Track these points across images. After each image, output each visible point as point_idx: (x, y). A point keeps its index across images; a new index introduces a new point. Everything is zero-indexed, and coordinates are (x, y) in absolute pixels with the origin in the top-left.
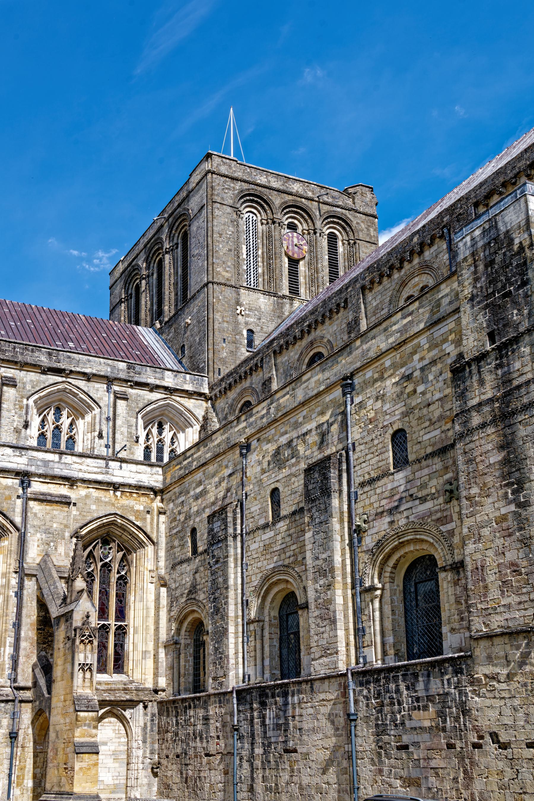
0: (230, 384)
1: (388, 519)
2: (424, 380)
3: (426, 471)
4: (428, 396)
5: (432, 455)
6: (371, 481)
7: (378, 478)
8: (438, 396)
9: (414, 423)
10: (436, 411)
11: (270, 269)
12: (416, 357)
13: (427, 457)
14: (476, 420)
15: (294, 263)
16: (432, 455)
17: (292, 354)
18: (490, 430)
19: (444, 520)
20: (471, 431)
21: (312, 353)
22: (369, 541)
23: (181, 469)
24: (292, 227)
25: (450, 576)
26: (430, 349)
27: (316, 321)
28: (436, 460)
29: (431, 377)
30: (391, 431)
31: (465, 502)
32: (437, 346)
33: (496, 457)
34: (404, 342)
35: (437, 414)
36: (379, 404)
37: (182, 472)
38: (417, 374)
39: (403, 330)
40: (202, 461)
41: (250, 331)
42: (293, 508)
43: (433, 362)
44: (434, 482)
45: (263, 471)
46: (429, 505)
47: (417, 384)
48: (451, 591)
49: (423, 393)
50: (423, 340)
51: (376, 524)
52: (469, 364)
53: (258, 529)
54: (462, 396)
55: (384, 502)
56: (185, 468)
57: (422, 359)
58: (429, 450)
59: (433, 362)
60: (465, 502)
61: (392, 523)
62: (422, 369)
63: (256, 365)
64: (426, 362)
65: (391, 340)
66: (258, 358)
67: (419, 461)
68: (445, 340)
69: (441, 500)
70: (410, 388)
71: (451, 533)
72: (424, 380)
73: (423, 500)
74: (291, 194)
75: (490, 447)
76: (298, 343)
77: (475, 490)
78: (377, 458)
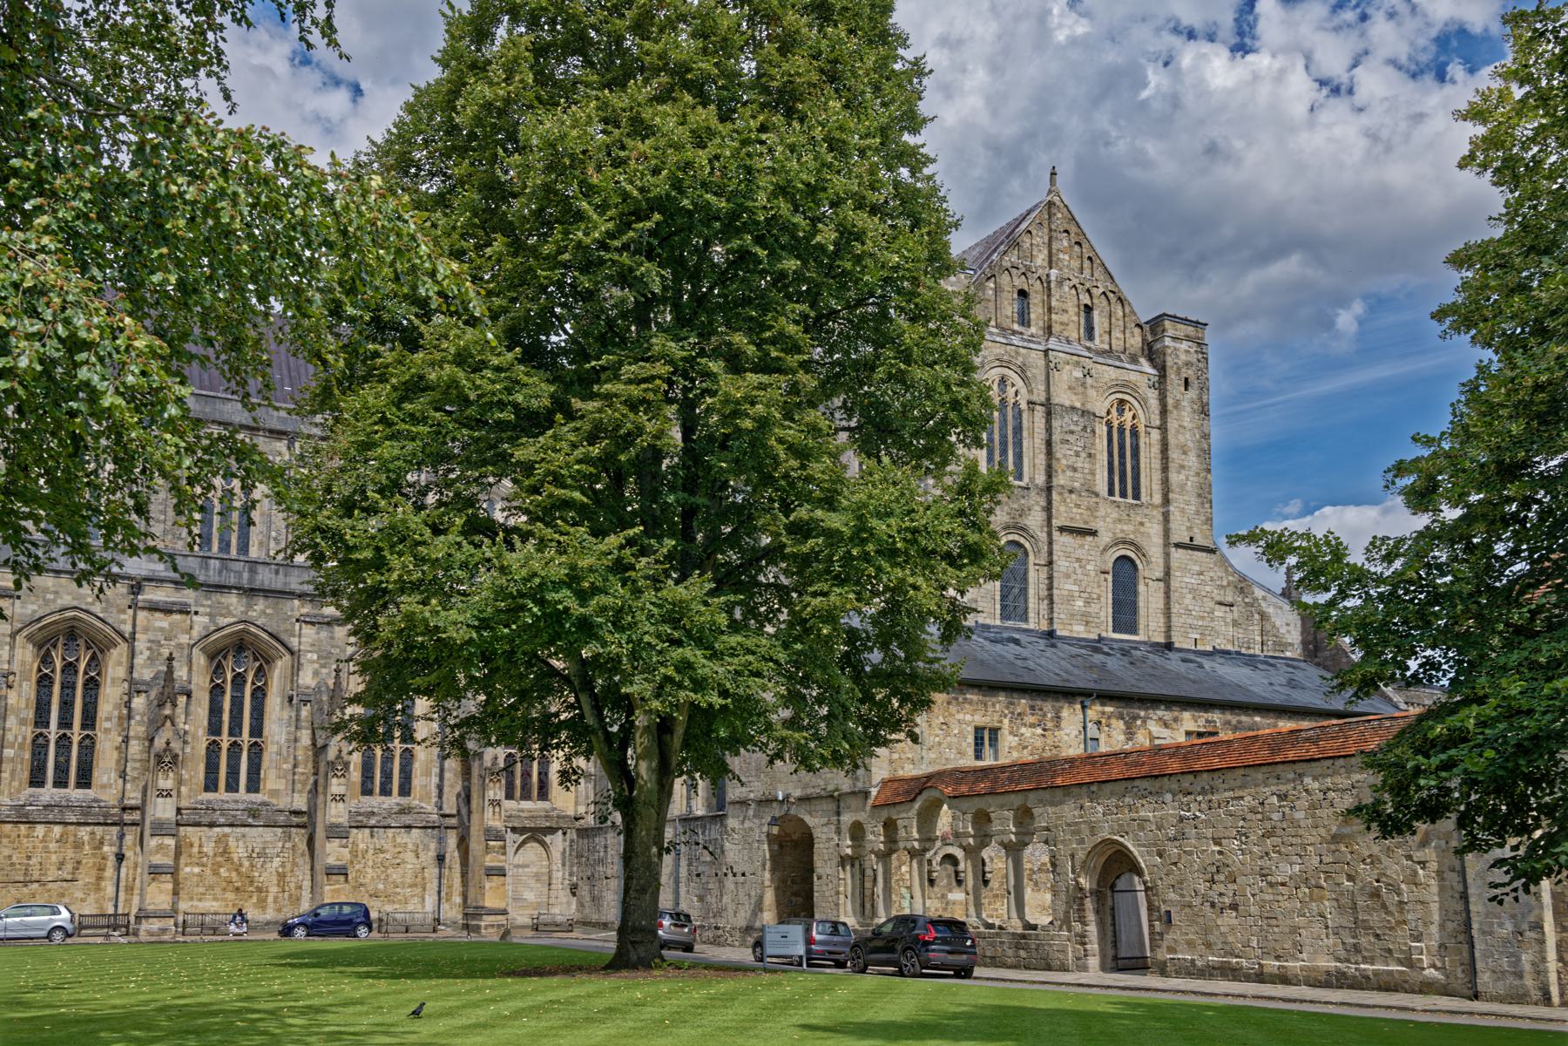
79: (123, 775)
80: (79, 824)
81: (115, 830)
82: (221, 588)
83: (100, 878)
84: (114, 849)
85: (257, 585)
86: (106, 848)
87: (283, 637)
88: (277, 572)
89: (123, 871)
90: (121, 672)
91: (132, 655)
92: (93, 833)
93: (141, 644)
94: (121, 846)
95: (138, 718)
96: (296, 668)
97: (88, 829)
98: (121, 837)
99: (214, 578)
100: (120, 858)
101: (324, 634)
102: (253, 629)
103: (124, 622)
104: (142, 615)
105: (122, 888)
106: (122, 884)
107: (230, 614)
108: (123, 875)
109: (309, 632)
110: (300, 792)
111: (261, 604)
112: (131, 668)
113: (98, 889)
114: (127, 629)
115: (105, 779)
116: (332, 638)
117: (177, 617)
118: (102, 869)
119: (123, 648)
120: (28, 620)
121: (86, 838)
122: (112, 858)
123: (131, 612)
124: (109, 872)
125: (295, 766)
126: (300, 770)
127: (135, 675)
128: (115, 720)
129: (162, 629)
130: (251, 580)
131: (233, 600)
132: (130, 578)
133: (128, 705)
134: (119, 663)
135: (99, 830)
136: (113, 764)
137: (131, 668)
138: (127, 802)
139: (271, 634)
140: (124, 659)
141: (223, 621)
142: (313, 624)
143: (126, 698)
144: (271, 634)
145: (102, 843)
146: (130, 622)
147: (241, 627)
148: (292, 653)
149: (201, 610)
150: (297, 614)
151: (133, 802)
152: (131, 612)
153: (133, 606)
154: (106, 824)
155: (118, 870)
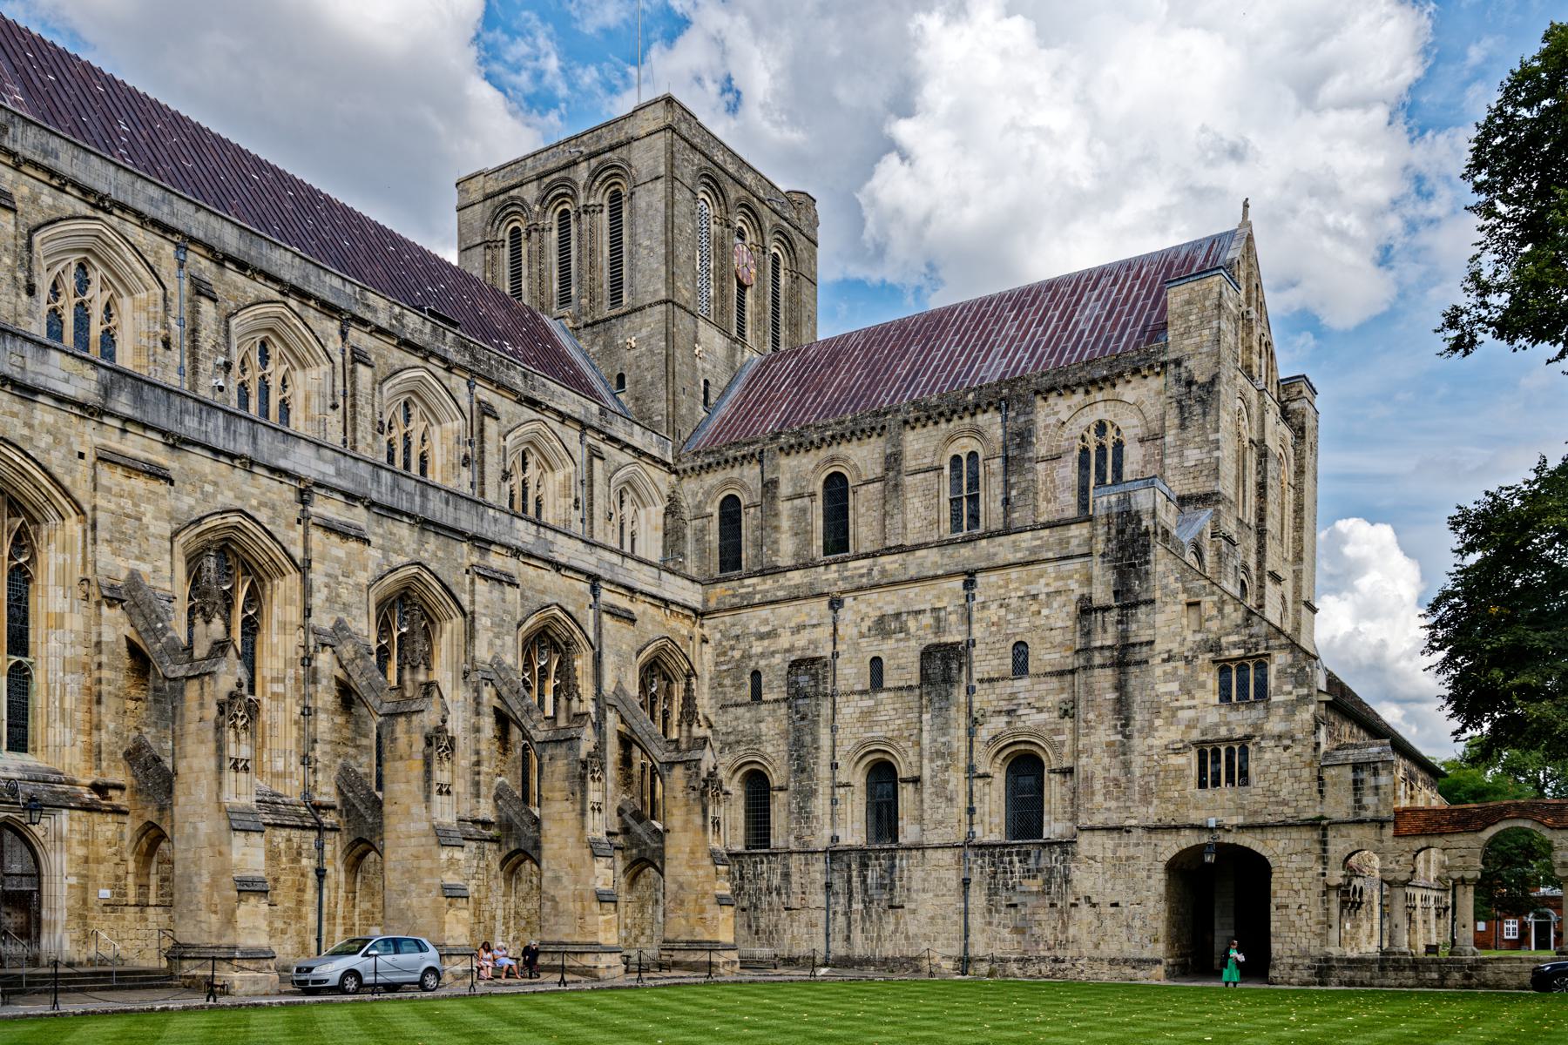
0: (709, 465)
1: (1005, 719)
2: (1049, 605)
3: (1044, 686)
4: (1052, 621)
5: (1051, 674)
6: (990, 680)
7: (997, 680)
8: (1060, 624)
9: (1036, 640)
10: (1057, 637)
11: (722, 294)
12: (1042, 581)
13: (1046, 674)
14: (1098, 659)
15: (742, 287)
16: (1051, 674)
17: (804, 461)
18: (1109, 671)
19: (1057, 732)
20: (1092, 667)
21: (831, 470)
22: (984, 733)
23: (734, 596)
24: (741, 235)
25: (1058, 777)
26: (1057, 579)
27: (843, 436)
28: (1054, 679)
29: (1055, 605)
30: (1013, 641)
31: (1082, 724)
32: (1062, 578)
33: (1112, 695)
34: (1032, 563)
35: (1059, 639)
36: (1002, 612)
37: (736, 600)
38: (1042, 597)
39: (1032, 550)
40: (770, 597)
41: (706, 382)
42: (901, 684)
43: (1058, 592)
44: (1050, 698)
45: (862, 636)
46: (1044, 716)
47: (1042, 605)
48: (1058, 789)
49: (1047, 617)
50: (1050, 567)
51: (994, 720)
52: (1096, 610)
53: (853, 693)
54: (1087, 634)
55: (1002, 703)
56: (743, 597)
57: (1047, 585)
58: (1049, 669)
59: (1058, 592)
60: (1082, 724)
61: (1009, 723)
62: (1048, 594)
63: (753, 455)
64: (1051, 589)
65: (1019, 555)
66: (758, 447)
67: (1038, 676)
68: (1071, 577)
69: (1056, 714)
70: (1035, 608)
71: (1062, 743)
72: (1049, 605)
73: (1040, 710)
74: (744, 187)
75: (1107, 685)
76: (813, 452)
77: (1091, 716)
78: (996, 662)
79: (306, 760)
80: (275, 825)
81: (313, 835)
82: (392, 512)
83: (300, 902)
84: (313, 863)
85: (429, 515)
86: (305, 862)
87: (455, 591)
88: (447, 503)
89: (325, 891)
90: (294, 614)
91: (307, 590)
92: (289, 840)
93: (317, 576)
94: (321, 859)
95: (324, 682)
96: (470, 635)
97: (285, 833)
98: (320, 848)
99: (387, 499)
100: (321, 874)
101: (496, 594)
102: (426, 575)
103: (293, 542)
104: (317, 535)
105: (324, 917)
106: (325, 910)
107: (400, 551)
108: (325, 899)
109: (479, 584)
110: (486, 797)
111: (432, 542)
112: (307, 612)
113: (299, 917)
114: (298, 553)
115: (280, 765)
116: (504, 600)
117: (353, 545)
118: (301, 890)
119: (293, 578)
120: (185, 519)
121: (282, 846)
122: (312, 875)
123: (300, 528)
124: (310, 895)
125: (478, 763)
126: (484, 768)
127: (313, 621)
128: (290, 683)
129: (338, 560)
130: (423, 507)
131: (403, 531)
132: (299, 479)
133: (307, 661)
134: (287, 601)
135: (296, 835)
136: (291, 744)
137: (307, 612)
138: (317, 798)
139: (445, 588)
140: (297, 596)
141: (398, 560)
142: (485, 578)
143: (301, 653)
144: (445, 588)
145: (299, 854)
146: (300, 543)
147: (414, 570)
148: (464, 614)
149: (373, 539)
150: (467, 563)
151: (325, 799)
152: (300, 528)
153: (303, 519)
154: (304, 828)
155: (320, 889)
